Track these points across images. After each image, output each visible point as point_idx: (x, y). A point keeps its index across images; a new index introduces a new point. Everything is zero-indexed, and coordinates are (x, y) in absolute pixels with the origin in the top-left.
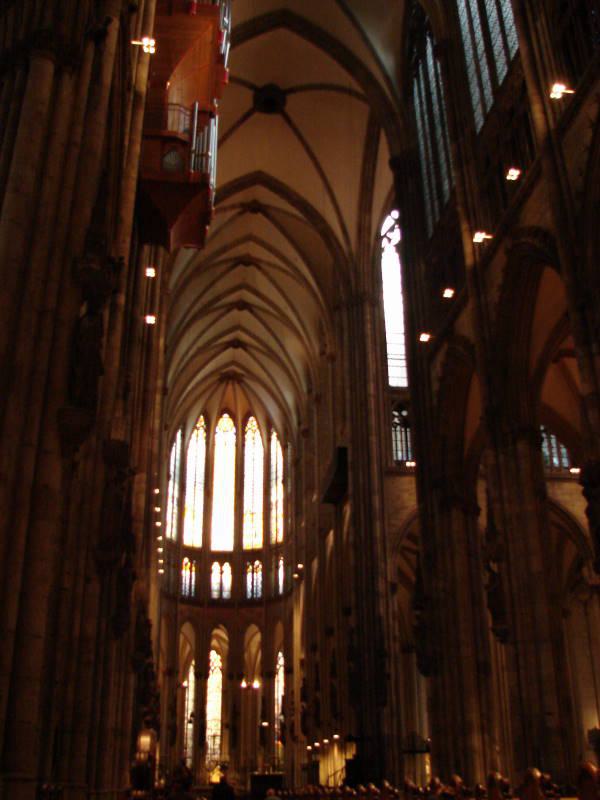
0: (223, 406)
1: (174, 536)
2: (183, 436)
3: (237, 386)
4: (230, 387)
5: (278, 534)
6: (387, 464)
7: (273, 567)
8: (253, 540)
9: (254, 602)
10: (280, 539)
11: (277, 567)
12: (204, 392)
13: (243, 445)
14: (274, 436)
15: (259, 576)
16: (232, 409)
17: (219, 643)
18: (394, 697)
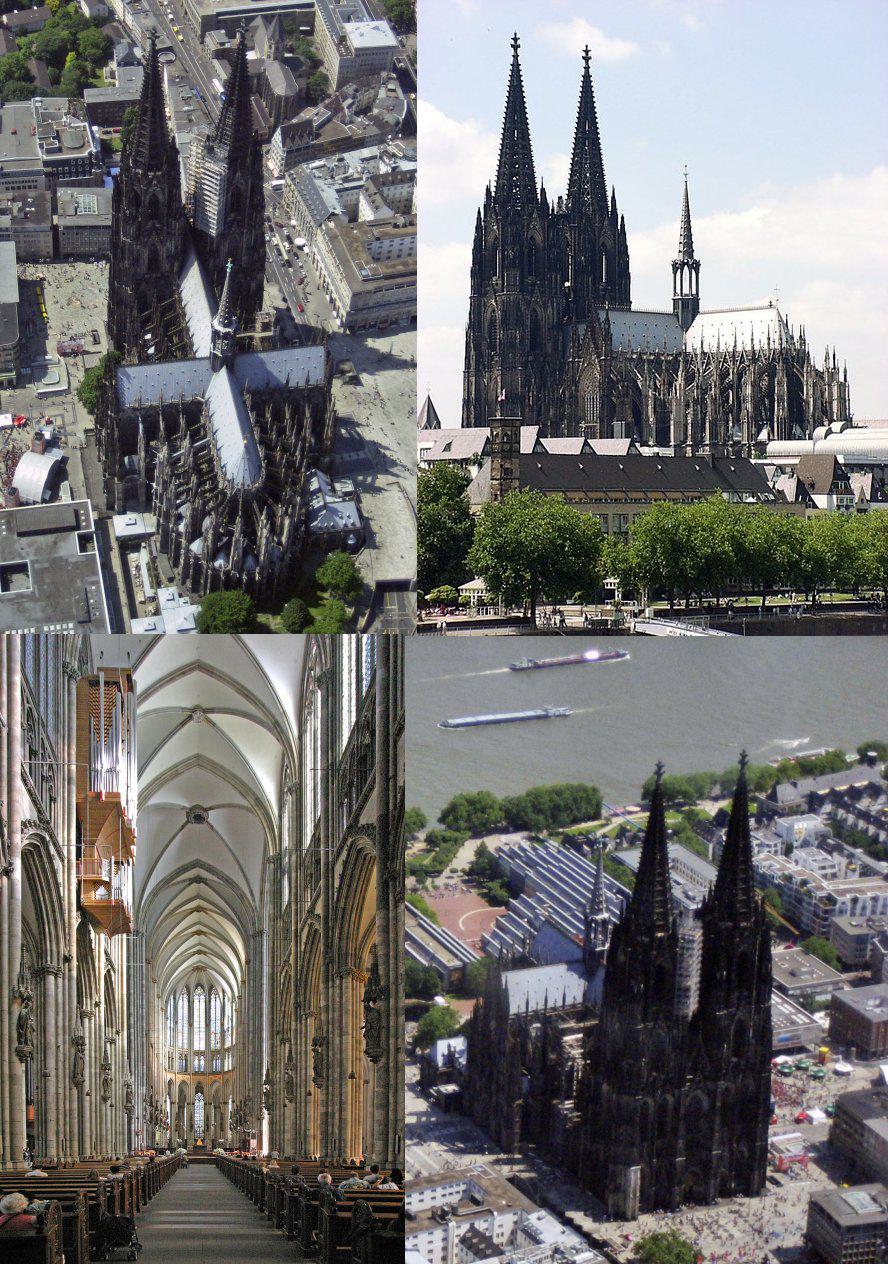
8: (215, 1044)
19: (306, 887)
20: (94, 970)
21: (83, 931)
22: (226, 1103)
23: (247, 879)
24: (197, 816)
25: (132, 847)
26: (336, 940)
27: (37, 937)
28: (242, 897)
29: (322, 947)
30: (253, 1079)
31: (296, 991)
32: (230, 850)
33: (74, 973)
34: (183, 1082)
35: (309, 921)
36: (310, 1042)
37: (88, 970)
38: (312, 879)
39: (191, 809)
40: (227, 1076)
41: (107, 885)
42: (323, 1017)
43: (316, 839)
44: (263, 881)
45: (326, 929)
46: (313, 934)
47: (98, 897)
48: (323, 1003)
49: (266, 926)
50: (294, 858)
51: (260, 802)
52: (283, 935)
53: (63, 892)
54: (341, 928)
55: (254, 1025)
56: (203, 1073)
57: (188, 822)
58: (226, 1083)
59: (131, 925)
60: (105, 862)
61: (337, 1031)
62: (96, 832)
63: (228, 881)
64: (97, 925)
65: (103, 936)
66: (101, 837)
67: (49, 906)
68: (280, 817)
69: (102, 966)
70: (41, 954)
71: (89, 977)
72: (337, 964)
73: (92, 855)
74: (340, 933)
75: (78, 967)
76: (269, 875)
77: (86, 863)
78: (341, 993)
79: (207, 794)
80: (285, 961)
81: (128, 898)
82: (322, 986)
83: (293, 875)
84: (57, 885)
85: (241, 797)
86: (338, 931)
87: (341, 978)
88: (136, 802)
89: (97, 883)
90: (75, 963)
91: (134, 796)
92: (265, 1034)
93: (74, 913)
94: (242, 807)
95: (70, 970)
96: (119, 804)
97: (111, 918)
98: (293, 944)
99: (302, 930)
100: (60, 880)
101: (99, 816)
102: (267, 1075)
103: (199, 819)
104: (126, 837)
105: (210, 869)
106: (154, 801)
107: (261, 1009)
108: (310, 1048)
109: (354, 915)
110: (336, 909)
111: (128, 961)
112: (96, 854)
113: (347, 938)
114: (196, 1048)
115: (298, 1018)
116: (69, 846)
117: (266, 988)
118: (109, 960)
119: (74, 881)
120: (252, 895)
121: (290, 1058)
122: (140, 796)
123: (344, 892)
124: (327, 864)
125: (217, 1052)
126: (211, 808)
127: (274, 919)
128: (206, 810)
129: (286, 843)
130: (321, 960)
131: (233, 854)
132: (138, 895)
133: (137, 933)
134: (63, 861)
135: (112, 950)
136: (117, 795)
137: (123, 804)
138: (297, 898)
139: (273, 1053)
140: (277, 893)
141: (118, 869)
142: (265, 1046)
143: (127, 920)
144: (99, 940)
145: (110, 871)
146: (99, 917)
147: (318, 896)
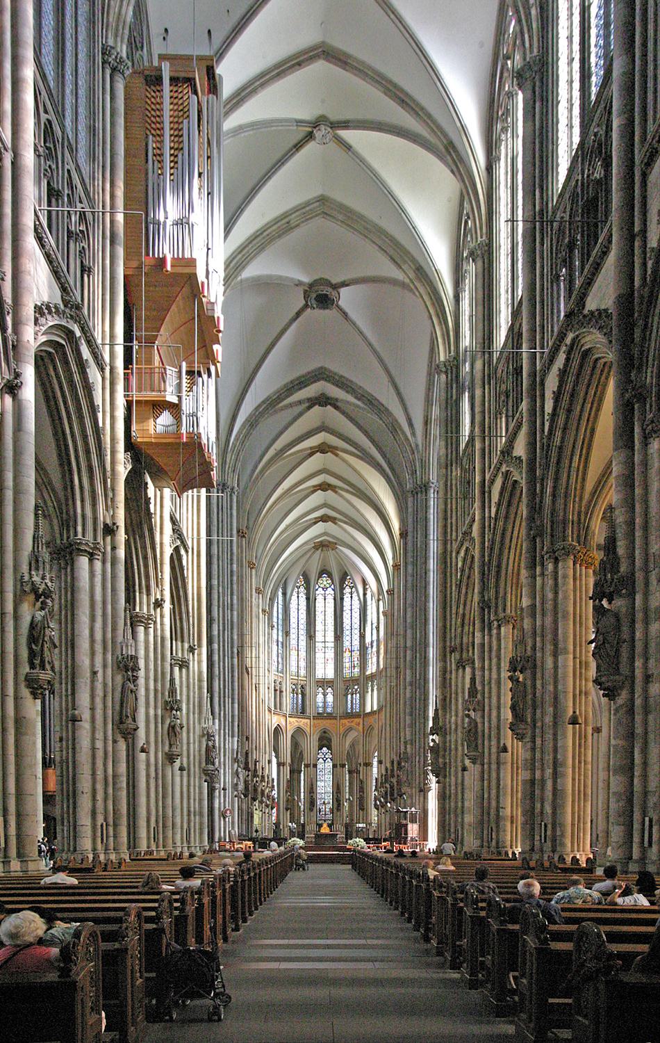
8: (351, 668)
11: (372, 690)
19: (498, 413)
20: (154, 549)
21: (135, 484)
22: (368, 764)
23: (399, 394)
24: (321, 296)
25: (216, 347)
26: (548, 500)
27: (61, 494)
28: (394, 428)
29: (524, 510)
30: (412, 725)
31: (482, 581)
32: (375, 352)
33: (121, 553)
34: (299, 731)
35: (504, 469)
36: (505, 665)
37: (144, 548)
38: (509, 399)
39: (311, 286)
40: (371, 720)
41: (175, 409)
42: (527, 624)
43: (515, 334)
44: (428, 402)
45: (532, 481)
46: (510, 488)
47: (160, 429)
48: (525, 602)
49: (433, 475)
50: (479, 365)
51: (423, 273)
52: (461, 491)
53: (103, 420)
54: (556, 479)
55: (414, 639)
56: (330, 716)
57: (306, 306)
58: (367, 732)
59: (214, 474)
60: (171, 372)
61: (549, 647)
62: (157, 322)
63: (372, 403)
64: (159, 474)
65: (167, 492)
66: (164, 332)
67: (79, 443)
68: (457, 298)
69: (165, 541)
70: (68, 522)
71: (145, 558)
72: (550, 538)
73: (149, 361)
74: (555, 488)
75: (127, 542)
76: (438, 393)
77: (139, 370)
78: (556, 585)
79: (335, 264)
80: (465, 534)
81: (208, 429)
82: (524, 573)
83: (478, 392)
84: (93, 409)
85: (393, 267)
86: (550, 484)
87: (556, 560)
88: (222, 274)
89: (159, 406)
90: (122, 536)
91: (218, 263)
92: (432, 653)
93: (121, 455)
94: (394, 282)
95: (114, 548)
96: (193, 276)
97: (181, 462)
98: (477, 505)
99: (492, 482)
100: (98, 401)
101: (162, 294)
102: (435, 719)
103: (324, 301)
104: (206, 331)
105: (342, 383)
106: (250, 272)
107: (426, 610)
108: (505, 674)
109: (576, 459)
110: (547, 448)
111: (209, 533)
112: (157, 358)
113: (566, 495)
114: (320, 674)
115: (486, 626)
116: (112, 345)
117: (433, 577)
118: (177, 532)
119: (121, 402)
120: (411, 425)
121: (473, 692)
122: (227, 266)
123: (561, 421)
124: (533, 374)
125: (354, 681)
126: (344, 284)
127: (447, 465)
128: (336, 287)
129: (466, 341)
130: (524, 532)
131: (381, 361)
132: (225, 426)
133: (223, 487)
134: (102, 370)
135: (180, 513)
136: (192, 262)
137: (201, 277)
138: (484, 430)
139: (444, 683)
140: (452, 423)
141: (192, 384)
142: (433, 672)
143: (206, 466)
144: (162, 500)
145: (179, 385)
146: (161, 460)
147: (519, 426)
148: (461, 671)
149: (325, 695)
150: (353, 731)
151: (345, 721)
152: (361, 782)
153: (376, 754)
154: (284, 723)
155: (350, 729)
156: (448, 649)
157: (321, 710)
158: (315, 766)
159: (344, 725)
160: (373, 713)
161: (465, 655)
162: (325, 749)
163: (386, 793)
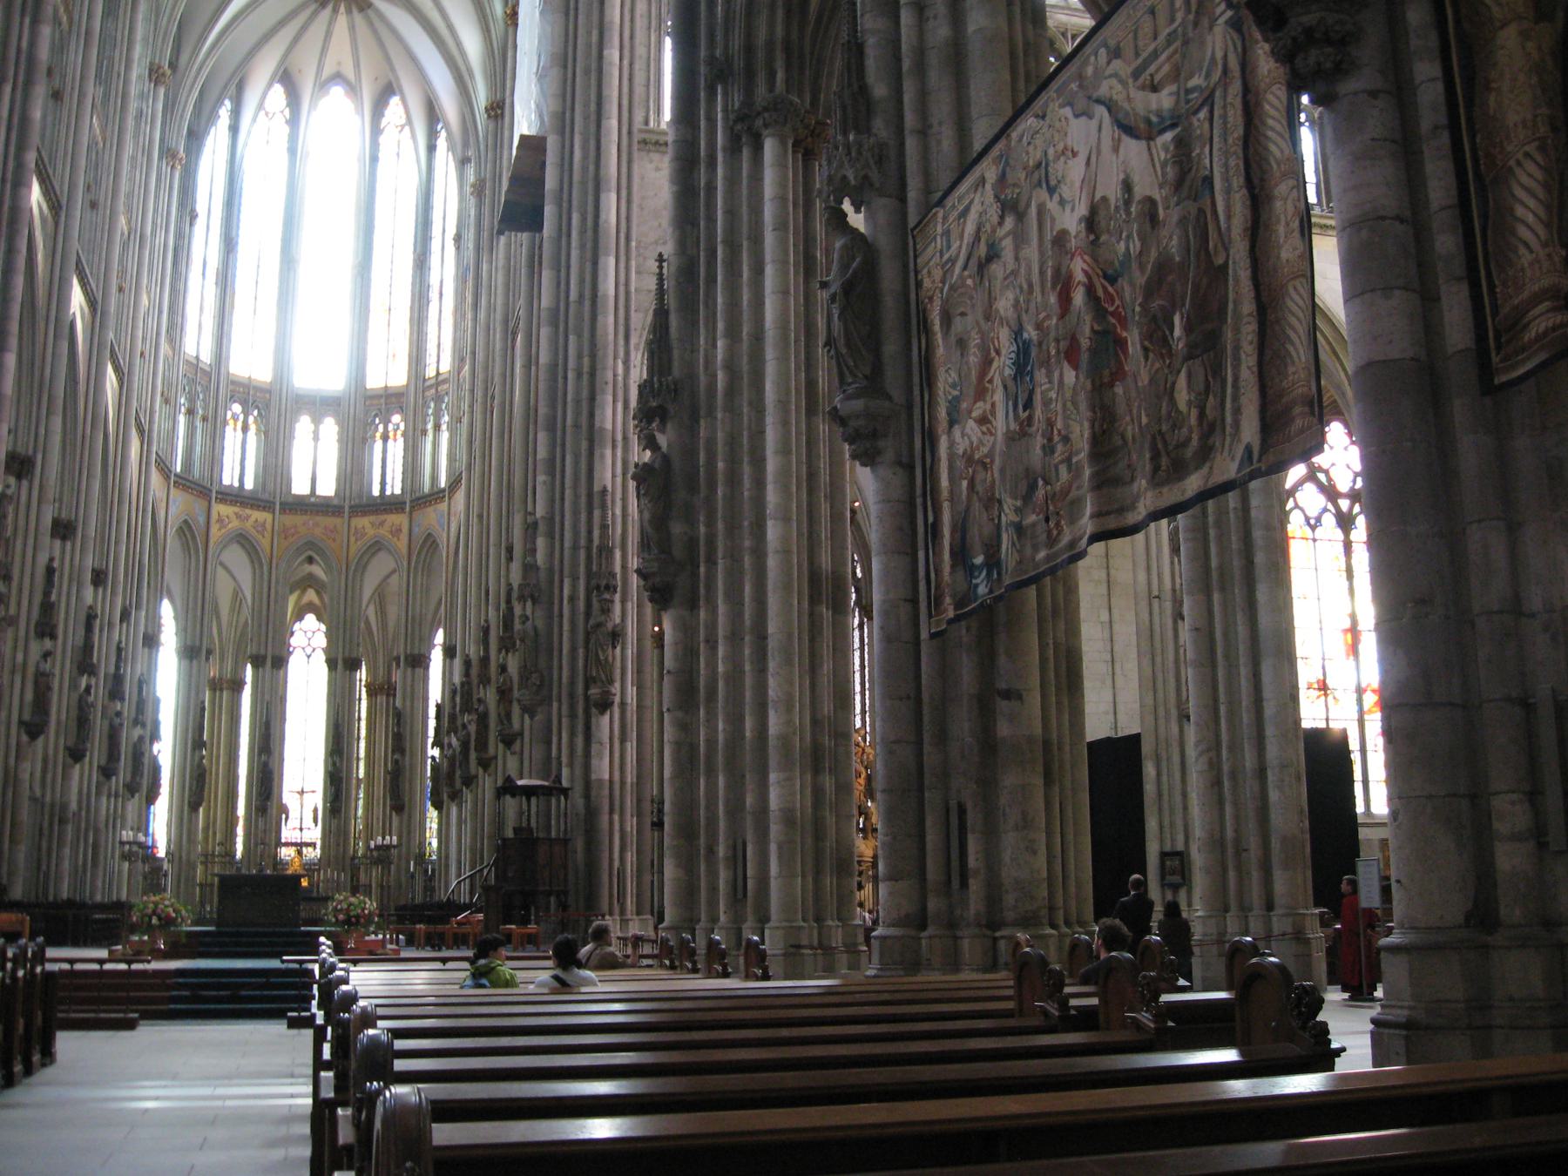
0: (328, 70)
1: (206, 357)
2: (234, 129)
3: (358, 18)
4: (342, 20)
5: (441, 358)
6: (647, 123)
7: (430, 426)
8: (388, 370)
9: (388, 505)
10: (445, 367)
11: (437, 427)
12: (282, 23)
13: (374, 159)
14: (442, 143)
15: (397, 449)
16: (349, 72)
17: (318, 593)
18: (631, 691)
22: (419, 662)
40: (431, 517)
148: (746, 153)
149: (316, 438)
150: (382, 555)
151: (363, 522)
152: (398, 715)
153: (439, 637)
154: (202, 520)
155: (376, 547)
156: (703, 69)
157: (300, 487)
158: (280, 662)
159: (360, 534)
160: (437, 496)
161: (761, 90)
162: (310, 620)
163: (465, 745)
